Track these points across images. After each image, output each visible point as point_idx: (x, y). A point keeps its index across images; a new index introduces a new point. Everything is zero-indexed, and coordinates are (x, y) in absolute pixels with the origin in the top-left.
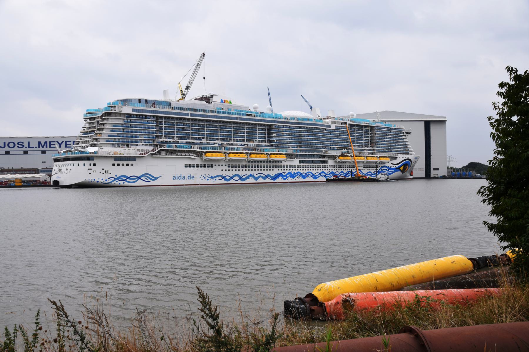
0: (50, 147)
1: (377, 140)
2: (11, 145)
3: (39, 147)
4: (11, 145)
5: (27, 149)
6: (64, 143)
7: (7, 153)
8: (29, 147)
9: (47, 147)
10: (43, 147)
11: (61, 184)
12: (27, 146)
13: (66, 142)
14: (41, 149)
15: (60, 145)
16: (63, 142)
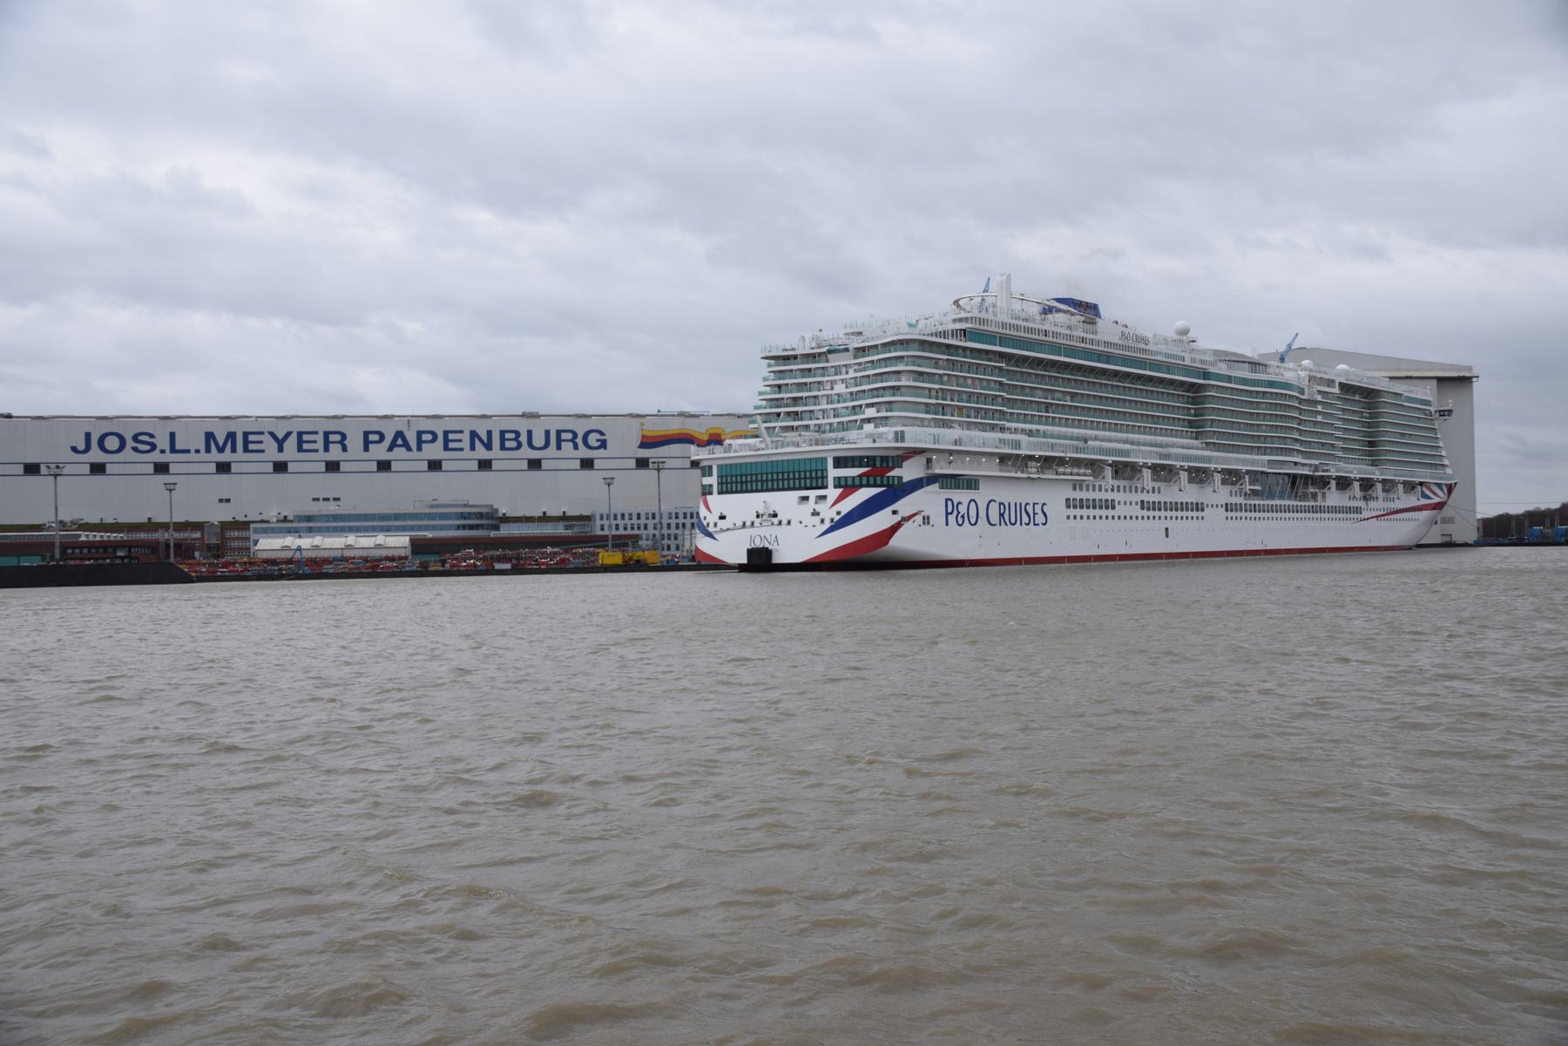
0: (246, 450)
1: (1388, 435)
2: (112, 443)
3: (208, 450)
4: (112, 443)
5: (168, 457)
6: (293, 438)
7: (98, 469)
8: (173, 450)
9: (234, 450)
10: (221, 450)
11: (778, 558)
12: (167, 449)
13: (300, 434)
14: (215, 456)
15: (280, 444)
16: (288, 434)
